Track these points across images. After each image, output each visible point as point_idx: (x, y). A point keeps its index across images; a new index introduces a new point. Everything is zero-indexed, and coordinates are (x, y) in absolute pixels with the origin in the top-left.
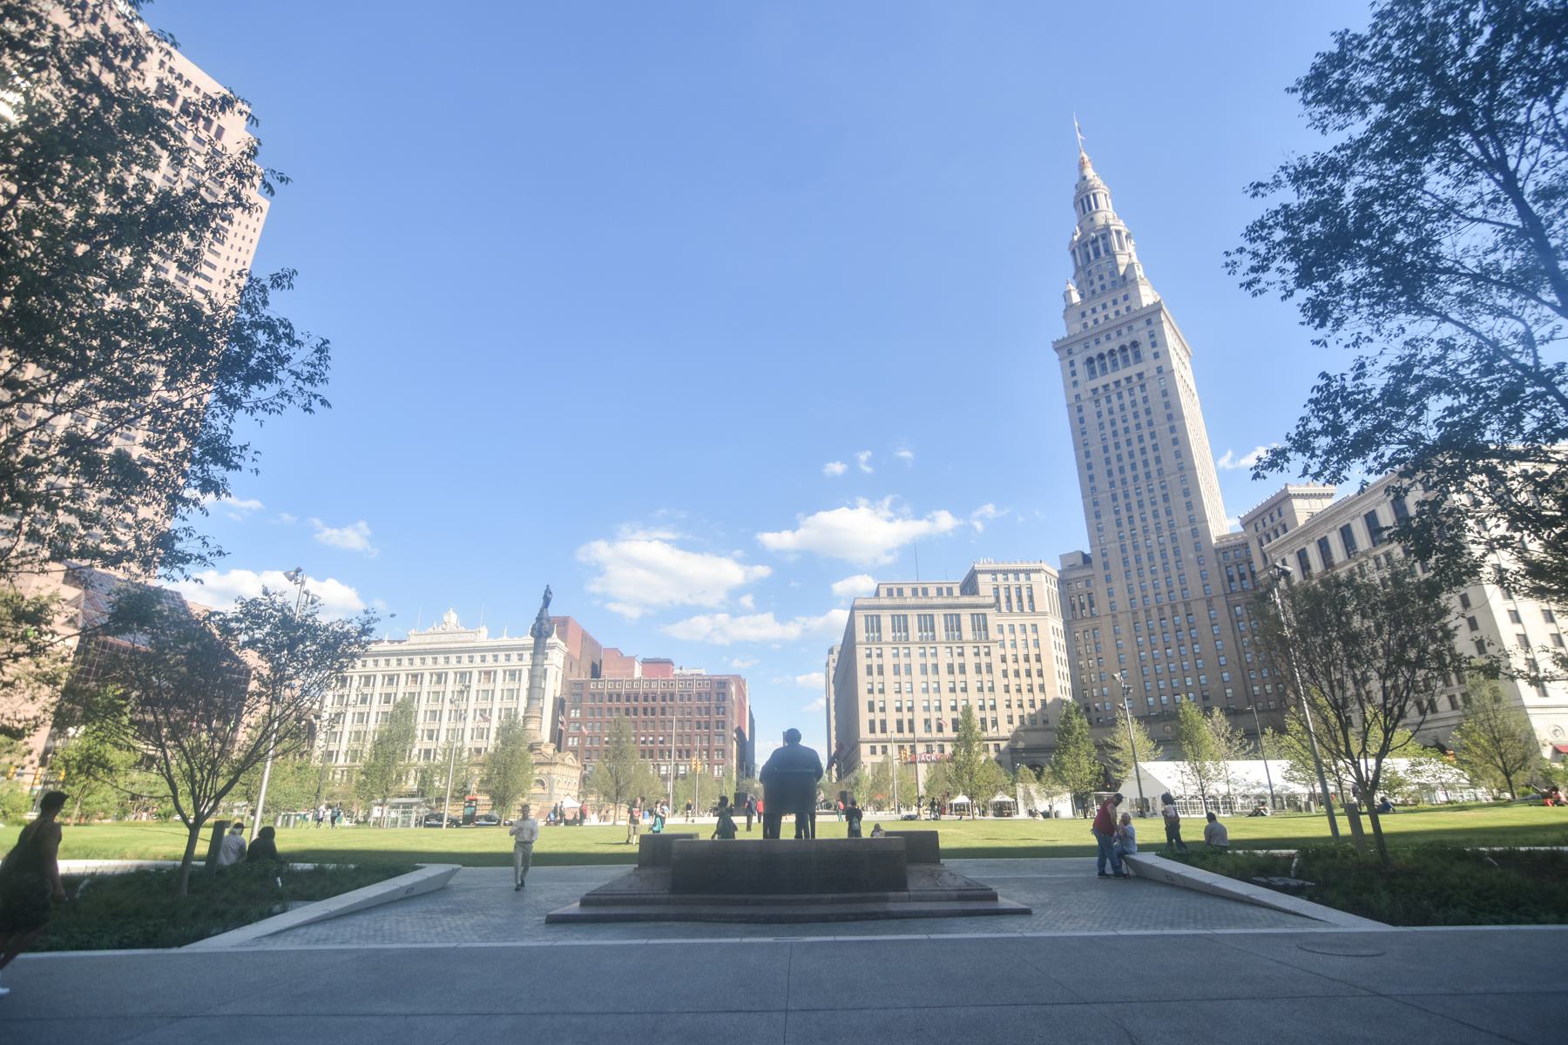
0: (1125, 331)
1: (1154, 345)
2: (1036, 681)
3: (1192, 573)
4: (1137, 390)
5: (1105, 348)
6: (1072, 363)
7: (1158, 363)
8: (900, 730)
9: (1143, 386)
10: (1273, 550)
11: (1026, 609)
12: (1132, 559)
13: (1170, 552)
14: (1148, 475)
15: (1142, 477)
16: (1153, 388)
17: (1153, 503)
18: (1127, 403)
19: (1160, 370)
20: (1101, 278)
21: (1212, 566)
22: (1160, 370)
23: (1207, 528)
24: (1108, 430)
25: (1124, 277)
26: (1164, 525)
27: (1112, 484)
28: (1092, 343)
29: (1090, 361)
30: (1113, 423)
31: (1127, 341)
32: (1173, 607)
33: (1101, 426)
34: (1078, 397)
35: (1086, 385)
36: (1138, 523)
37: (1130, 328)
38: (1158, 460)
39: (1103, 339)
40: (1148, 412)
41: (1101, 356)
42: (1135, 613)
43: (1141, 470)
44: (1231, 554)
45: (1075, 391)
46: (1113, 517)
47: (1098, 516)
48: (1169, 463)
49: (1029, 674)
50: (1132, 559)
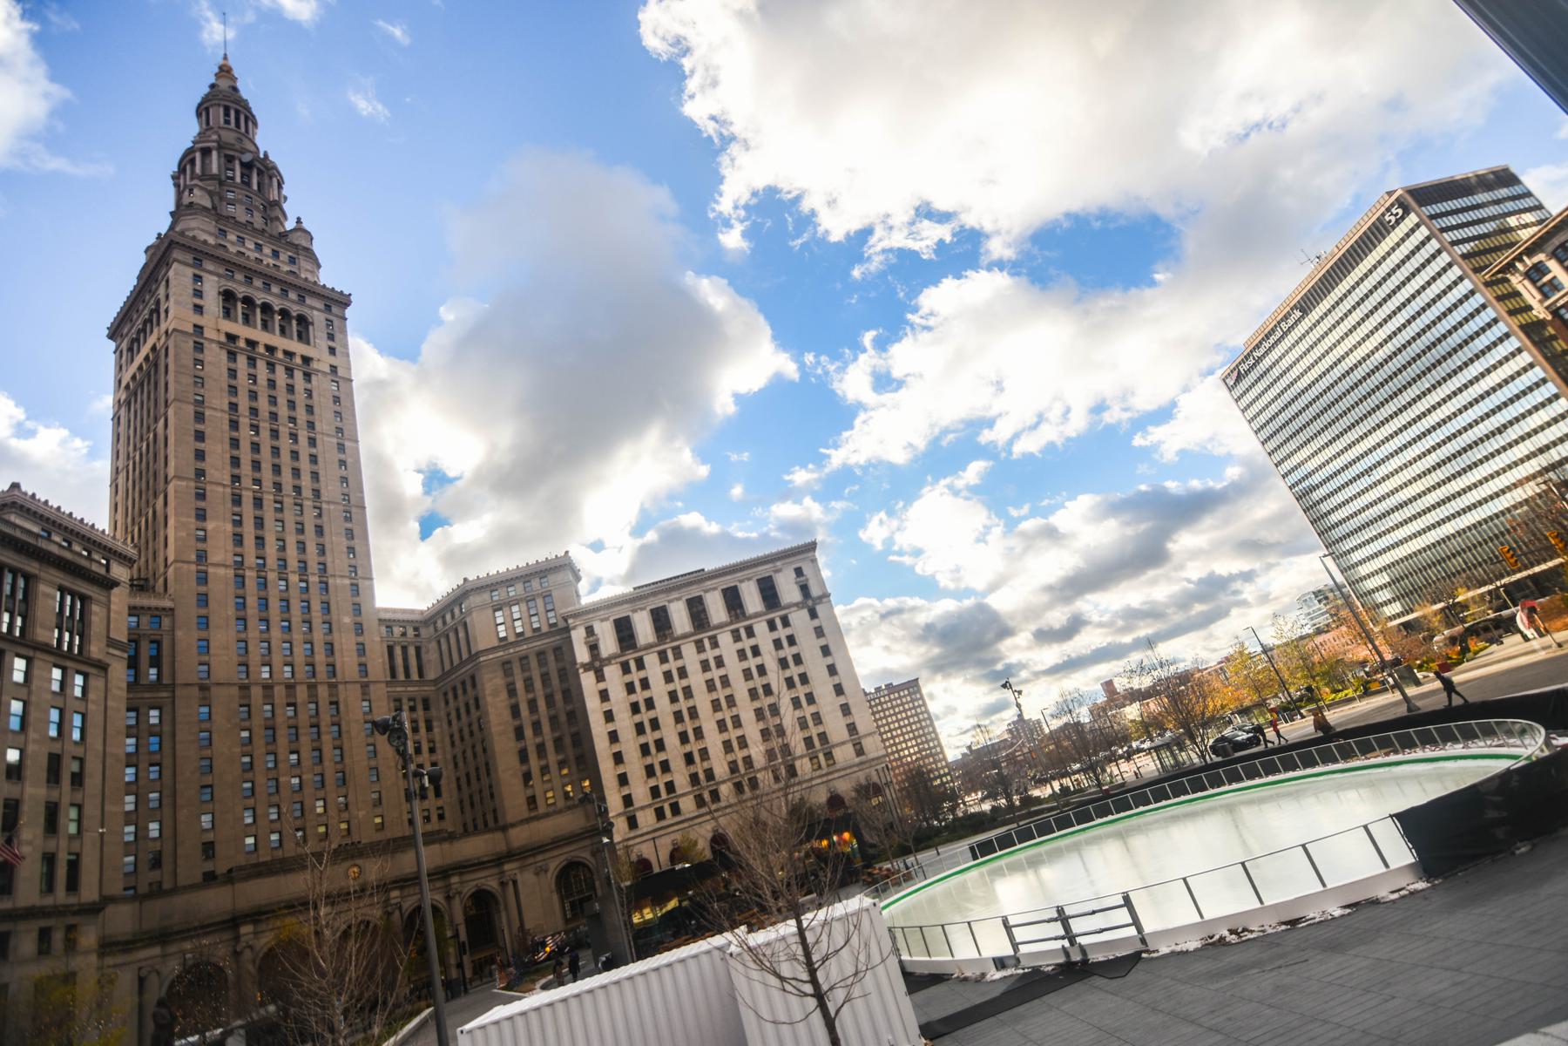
0: (293, 295)
1: (331, 337)
4: (298, 375)
5: (260, 298)
10: (575, 616)
12: (252, 601)
13: (316, 606)
16: (321, 384)
17: (301, 531)
22: (334, 369)
23: (371, 588)
24: (243, 402)
25: (284, 235)
26: (313, 566)
28: (239, 277)
29: (228, 296)
30: (253, 395)
32: (312, 687)
34: (199, 329)
35: (215, 324)
37: (302, 299)
41: (248, 301)
42: (244, 688)
44: (397, 631)
46: (229, 527)
47: (201, 515)
50: (252, 601)
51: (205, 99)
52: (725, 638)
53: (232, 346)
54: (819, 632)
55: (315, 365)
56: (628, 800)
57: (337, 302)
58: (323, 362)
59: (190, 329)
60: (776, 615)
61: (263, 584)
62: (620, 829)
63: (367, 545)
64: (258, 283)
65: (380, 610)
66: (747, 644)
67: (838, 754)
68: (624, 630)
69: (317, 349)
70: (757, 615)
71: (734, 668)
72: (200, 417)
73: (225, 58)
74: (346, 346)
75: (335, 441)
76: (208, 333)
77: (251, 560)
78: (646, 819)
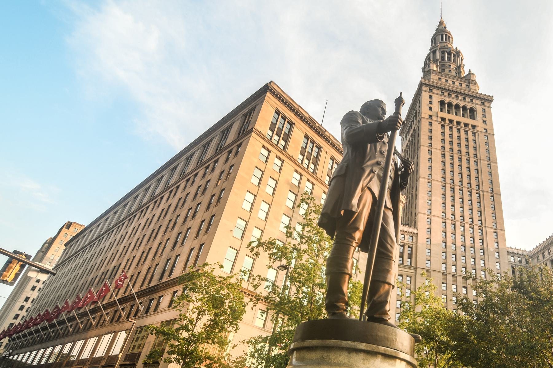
4: (470, 133)
5: (455, 102)
6: (431, 97)
7: (486, 127)
9: (474, 133)
20: (450, 71)
25: (464, 77)
28: (446, 94)
29: (442, 103)
31: (469, 106)
33: (443, 141)
37: (472, 100)
39: (453, 96)
40: (475, 148)
41: (450, 105)
45: (431, 113)
51: (434, 35)
53: (443, 123)
55: (478, 129)
58: (480, 126)
59: (428, 117)
63: (502, 213)
64: (453, 96)
69: (479, 122)
72: (430, 152)
75: (486, 163)
76: (434, 118)
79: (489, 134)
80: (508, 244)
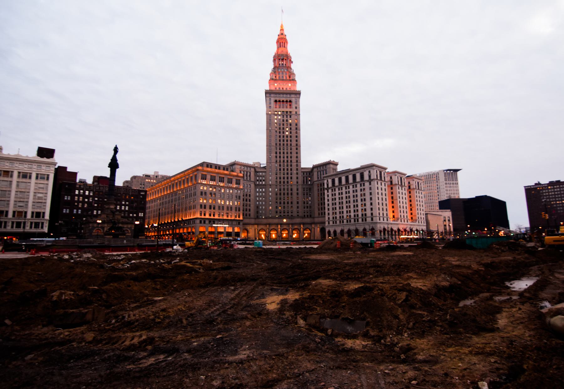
2: (248, 202)
3: (294, 176)
5: (281, 100)
7: (296, 110)
8: (210, 215)
11: (248, 179)
14: (287, 144)
15: (285, 145)
18: (285, 120)
19: (296, 112)
21: (300, 176)
22: (296, 112)
26: (289, 161)
27: (276, 144)
36: (282, 159)
38: (291, 141)
43: (285, 143)
46: (275, 155)
48: (294, 143)
49: (246, 201)
52: (351, 187)
54: (370, 189)
56: (329, 218)
57: (298, 94)
60: (362, 183)
61: (280, 165)
62: (327, 223)
65: (302, 168)
66: (355, 189)
67: (367, 219)
68: (333, 181)
69: (293, 110)
70: (358, 182)
71: (351, 194)
73: (282, 30)
74: (299, 105)
77: (278, 161)
78: (331, 223)
79: (297, 114)
80: (302, 167)
